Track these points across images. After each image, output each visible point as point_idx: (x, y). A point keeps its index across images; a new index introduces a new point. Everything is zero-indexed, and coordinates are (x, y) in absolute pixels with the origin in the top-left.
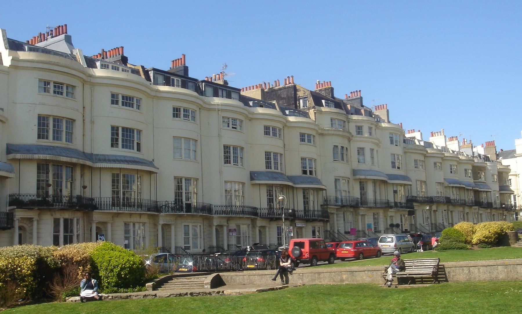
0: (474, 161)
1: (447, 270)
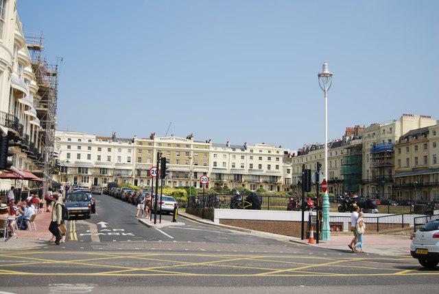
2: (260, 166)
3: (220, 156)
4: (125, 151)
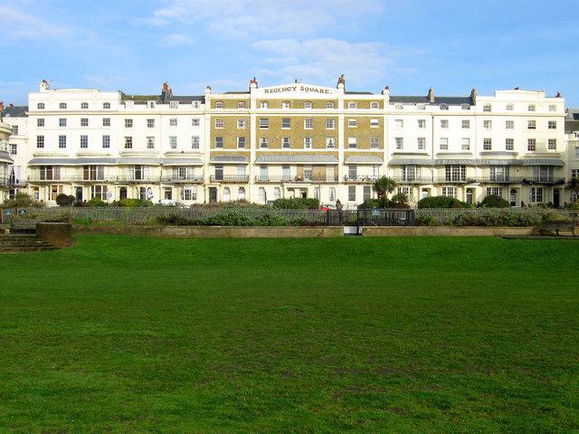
4: (185, 122)
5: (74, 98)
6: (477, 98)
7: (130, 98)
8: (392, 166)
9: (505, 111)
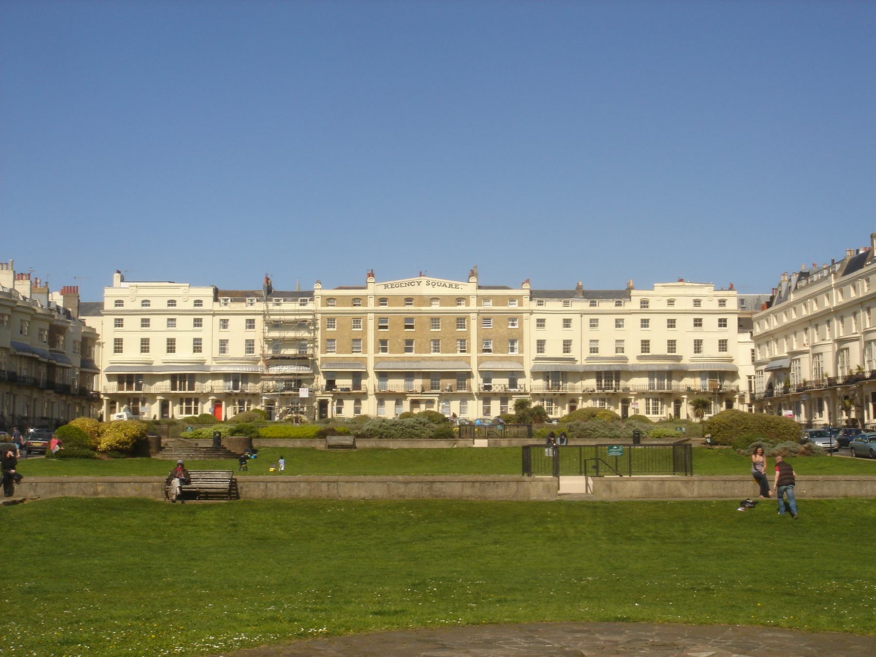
0: (54, 317)
1: (239, 485)
2: (672, 344)
3: (554, 323)
5: (158, 294)
6: (633, 292)
7: (226, 294)
8: (535, 375)
9: (664, 306)
